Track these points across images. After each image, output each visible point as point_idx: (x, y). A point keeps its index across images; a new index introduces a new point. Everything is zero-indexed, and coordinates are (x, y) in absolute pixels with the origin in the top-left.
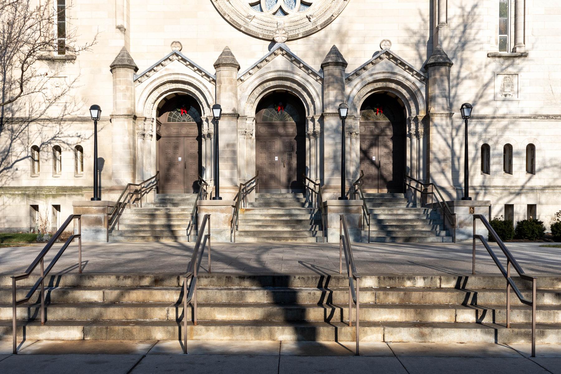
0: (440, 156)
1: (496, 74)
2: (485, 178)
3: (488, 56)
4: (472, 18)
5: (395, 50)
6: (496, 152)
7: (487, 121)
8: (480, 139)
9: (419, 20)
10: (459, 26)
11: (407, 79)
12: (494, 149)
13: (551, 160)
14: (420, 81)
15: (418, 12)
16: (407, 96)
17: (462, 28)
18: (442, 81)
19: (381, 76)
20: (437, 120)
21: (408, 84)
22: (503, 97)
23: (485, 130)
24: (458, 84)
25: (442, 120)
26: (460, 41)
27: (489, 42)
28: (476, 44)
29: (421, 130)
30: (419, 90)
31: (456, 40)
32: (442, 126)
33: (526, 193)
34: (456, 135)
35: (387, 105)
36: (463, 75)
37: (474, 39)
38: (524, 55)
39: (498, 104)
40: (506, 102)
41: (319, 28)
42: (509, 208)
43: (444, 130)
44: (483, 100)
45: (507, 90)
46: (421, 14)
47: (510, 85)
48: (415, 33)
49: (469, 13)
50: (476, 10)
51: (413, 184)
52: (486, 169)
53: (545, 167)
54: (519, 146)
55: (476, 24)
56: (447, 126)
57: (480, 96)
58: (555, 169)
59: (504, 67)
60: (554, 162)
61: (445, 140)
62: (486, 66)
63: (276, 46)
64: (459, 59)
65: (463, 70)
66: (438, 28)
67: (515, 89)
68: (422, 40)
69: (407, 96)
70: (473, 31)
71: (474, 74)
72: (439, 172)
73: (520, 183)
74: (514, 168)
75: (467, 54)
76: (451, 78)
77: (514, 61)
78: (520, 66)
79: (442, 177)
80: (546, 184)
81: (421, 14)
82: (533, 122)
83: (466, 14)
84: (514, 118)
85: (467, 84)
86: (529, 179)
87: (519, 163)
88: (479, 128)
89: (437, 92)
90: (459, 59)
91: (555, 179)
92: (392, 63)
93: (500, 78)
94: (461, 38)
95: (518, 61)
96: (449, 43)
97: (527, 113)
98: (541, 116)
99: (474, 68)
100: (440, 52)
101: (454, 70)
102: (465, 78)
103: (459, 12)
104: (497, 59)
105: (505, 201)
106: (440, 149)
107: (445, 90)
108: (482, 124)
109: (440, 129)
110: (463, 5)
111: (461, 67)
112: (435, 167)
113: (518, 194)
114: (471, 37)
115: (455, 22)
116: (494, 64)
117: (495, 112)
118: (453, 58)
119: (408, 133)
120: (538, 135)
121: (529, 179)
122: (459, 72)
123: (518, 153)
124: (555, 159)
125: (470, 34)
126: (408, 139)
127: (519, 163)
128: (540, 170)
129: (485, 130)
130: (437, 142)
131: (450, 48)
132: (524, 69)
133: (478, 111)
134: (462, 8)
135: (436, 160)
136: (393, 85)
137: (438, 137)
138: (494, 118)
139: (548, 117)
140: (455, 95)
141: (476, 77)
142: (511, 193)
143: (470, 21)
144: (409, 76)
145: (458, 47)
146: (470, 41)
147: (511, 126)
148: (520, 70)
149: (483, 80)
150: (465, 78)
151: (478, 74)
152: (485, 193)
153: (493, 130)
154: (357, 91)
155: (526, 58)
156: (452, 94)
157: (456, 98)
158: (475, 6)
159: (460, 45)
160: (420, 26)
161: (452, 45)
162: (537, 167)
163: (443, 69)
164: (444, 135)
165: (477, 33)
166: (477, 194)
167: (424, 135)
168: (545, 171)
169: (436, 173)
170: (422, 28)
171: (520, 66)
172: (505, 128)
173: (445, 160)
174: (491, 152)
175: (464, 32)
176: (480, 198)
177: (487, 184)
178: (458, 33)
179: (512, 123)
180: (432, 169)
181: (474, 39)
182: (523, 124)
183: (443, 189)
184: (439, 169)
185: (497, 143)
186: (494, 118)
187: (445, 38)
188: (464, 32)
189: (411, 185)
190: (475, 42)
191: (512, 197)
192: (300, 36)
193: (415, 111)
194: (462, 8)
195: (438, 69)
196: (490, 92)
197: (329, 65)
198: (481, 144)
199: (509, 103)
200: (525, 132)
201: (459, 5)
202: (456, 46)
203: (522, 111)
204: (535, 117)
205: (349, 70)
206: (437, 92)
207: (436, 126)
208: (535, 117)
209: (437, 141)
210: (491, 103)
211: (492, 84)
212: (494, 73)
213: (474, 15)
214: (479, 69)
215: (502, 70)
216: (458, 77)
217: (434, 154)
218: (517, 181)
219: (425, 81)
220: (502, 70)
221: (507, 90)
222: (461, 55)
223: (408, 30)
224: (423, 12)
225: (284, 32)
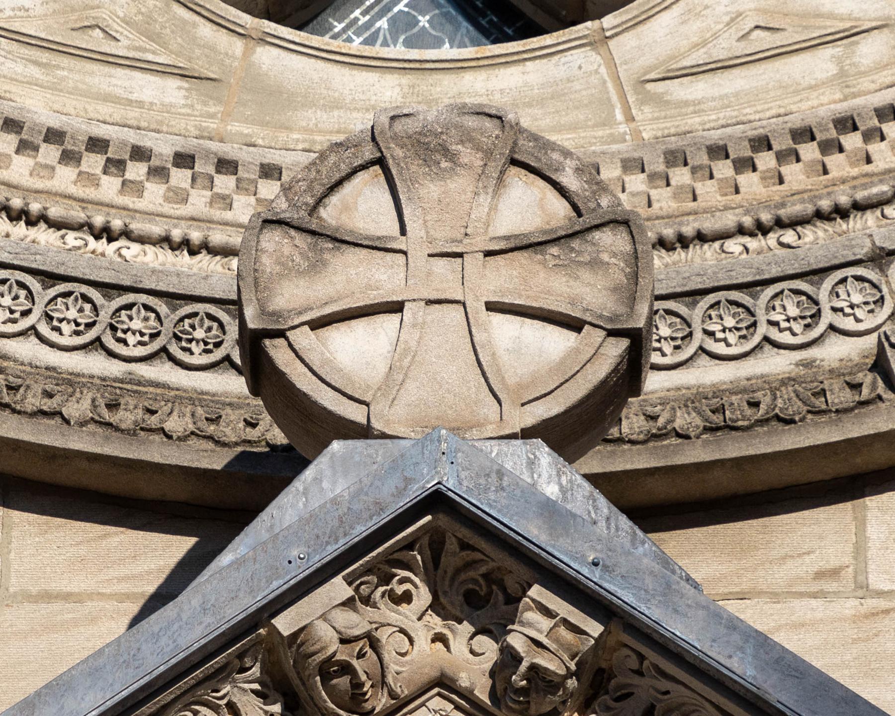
63: (328, 495)
225: (526, 206)
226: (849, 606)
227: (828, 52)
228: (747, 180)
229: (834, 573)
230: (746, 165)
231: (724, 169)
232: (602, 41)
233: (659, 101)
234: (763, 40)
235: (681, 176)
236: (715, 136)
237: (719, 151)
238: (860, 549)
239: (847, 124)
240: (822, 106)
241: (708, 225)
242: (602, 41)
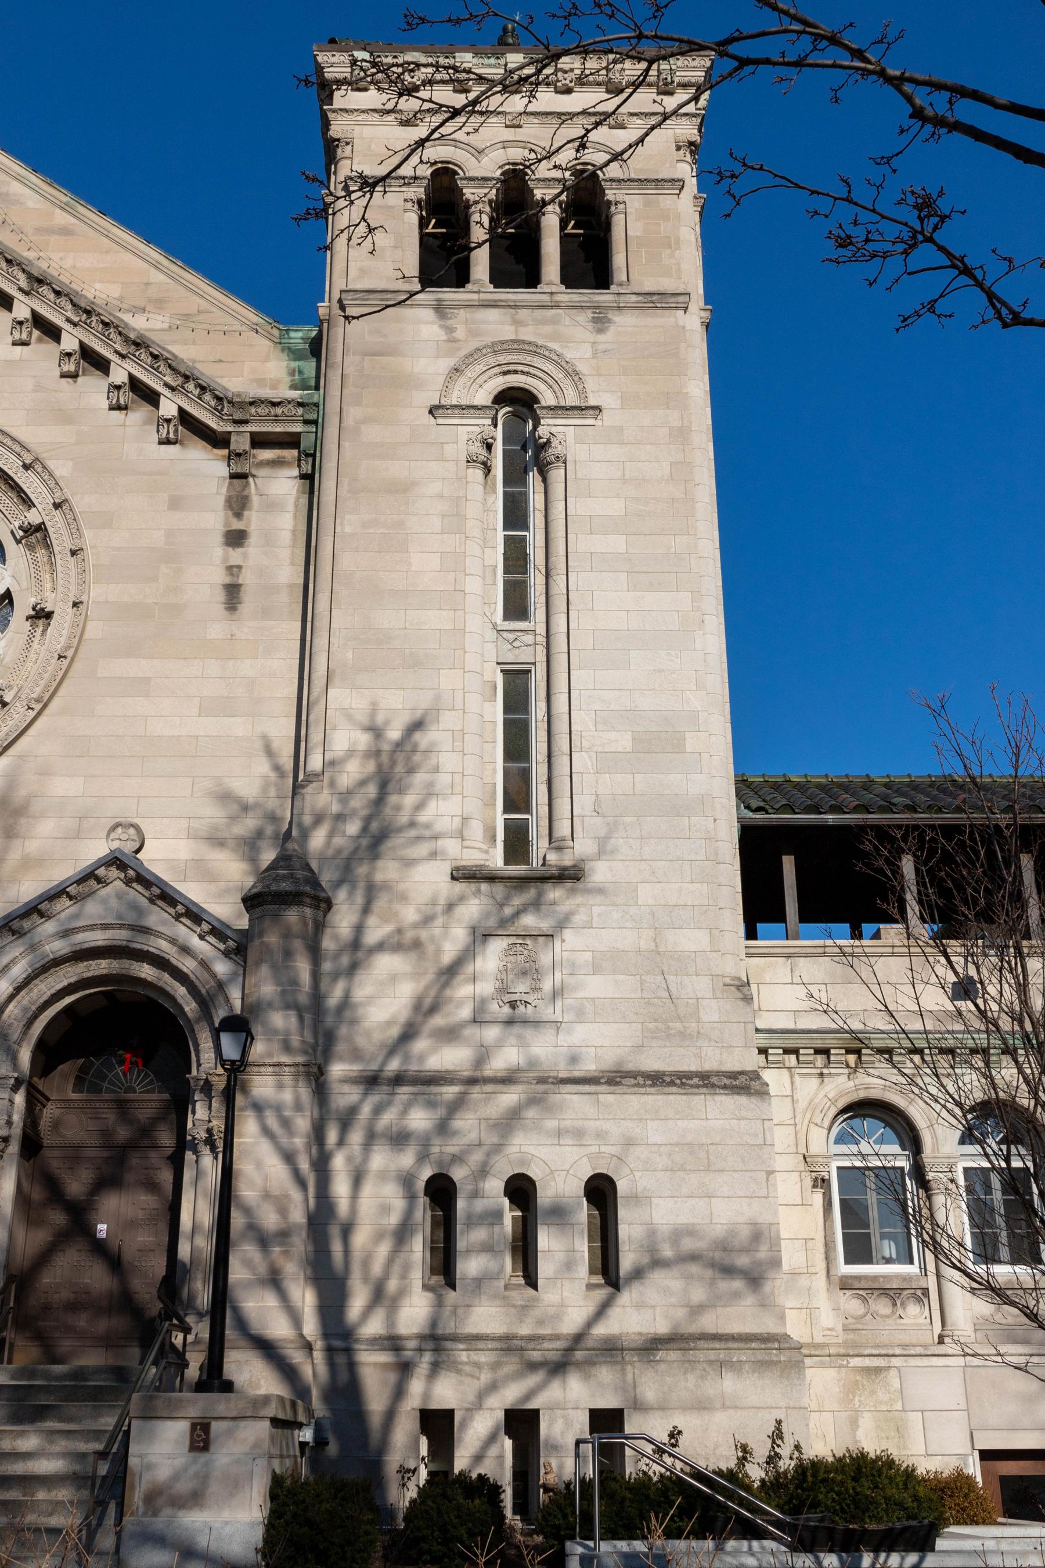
0: (270, 1220)
1: (481, 936)
2: (439, 1303)
3: (453, 878)
4: (408, 759)
5: (159, 857)
6: (480, 1205)
7: (450, 1091)
8: (423, 1157)
10: (363, 783)
12: (475, 1194)
13: (677, 1234)
14: (227, 954)
15: (259, 744)
16: (190, 1007)
17: (372, 791)
18: (288, 954)
19: (97, 938)
20: (261, 1085)
22: (506, 1009)
23: (443, 1128)
24: (353, 968)
25: (280, 1086)
26: (365, 829)
27: (460, 835)
28: (419, 838)
30: (221, 986)
31: (353, 828)
32: (278, 1108)
33: (590, 1363)
34: (341, 1143)
36: (374, 934)
37: (412, 824)
38: (570, 876)
39: (491, 1033)
40: (516, 1029)
42: (522, 1424)
43: (286, 1123)
44: (438, 1021)
45: (521, 987)
47: (530, 971)
48: (245, 808)
49: (399, 745)
50: (417, 736)
52: (444, 1265)
53: (658, 1263)
54: (561, 1179)
55: (419, 779)
56: (298, 1107)
57: (425, 1008)
58: (694, 1268)
59: (508, 911)
60: (688, 1245)
61: (289, 1157)
62: (450, 907)
65: (372, 921)
67: (547, 985)
68: (269, 830)
69: (190, 1007)
70: (409, 800)
71: (409, 935)
73: (572, 1321)
74: (545, 1268)
75: (387, 870)
76: (328, 944)
77: (540, 895)
78: (563, 908)
79: (270, 1300)
80: (662, 1328)
81: (269, 752)
82: (608, 1098)
83: (386, 747)
84: (542, 1081)
85: (385, 964)
86: (602, 1311)
87: (563, 1249)
88: (419, 1120)
89: (267, 989)
90: (362, 885)
91: (696, 1310)
92: (137, 895)
93: (497, 946)
94: (368, 820)
95: (554, 893)
97: (589, 1066)
98: (633, 1075)
99: (410, 914)
101: (343, 919)
102: (380, 947)
103: (363, 740)
104: (484, 887)
105: (510, 1395)
106: (267, 1195)
107: (295, 982)
108: (431, 1104)
109: (272, 1122)
110: (380, 719)
111: (366, 910)
112: (248, 1263)
113: (558, 1368)
114: (403, 819)
115: (352, 772)
116: (474, 907)
117: (480, 1061)
118: (338, 884)
120: (629, 1143)
121: (602, 1311)
122: (359, 929)
123: (559, 1213)
124: (690, 1231)
125: (398, 808)
127: (563, 1249)
128: (638, 1274)
129: (443, 1128)
130: (263, 1168)
131: (330, 852)
132: (578, 919)
133: (422, 1058)
134: (376, 731)
136: (146, 971)
137: (266, 1151)
138: (472, 1081)
139: (657, 1079)
140: (346, 1003)
141: (417, 945)
142: (533, 1366)
143: (399, 768)
144: (195, 942)
145: (356, 850)
146: (400, 830)
147: (531, 1113)
148: (562, 924)
149: (438, 952)
150: (380, 947)
151: (424, 934)
152: (435, 1368)
153: (468, 1125)
155: (580, 885)
156: (333, 1000)
157: (347, 1014)
158: (417, 726)
159: (365, 842)
160: (265, 789)
161: (338, 841)
162: (627, 1261)
163: (292, 916)
164: (284, 1140)
165: (420, 807)
166: (405, 1369)
168: (659, 1278)
169: (248, 1285)
170: (272, 792)
171: (563, 908)
172: (512, 1119)
173: (284, 1235)
174: (461, 1204)
175: (380, 801)
176: (416, 1386)
177: (448, 1327)
178: (358, 804)
179: (533, 1101)
180: (237, 1272)
181: (412, 824)
182: (575, 1104)
184: (262, 1269)
185: (483, 1172)
186: (472, 1081)
187: (318, 820)
188: (380, 801)
190: (413, 833)
191: (533, 1380)
194: (376, 731)
195: (276, 916)
196: (464, 994)
198: (427, 1173)
199: (529, 1033)
200: (578, 1134)
201: (365, 721)
202: (351, 846)
203: (574, 1059)
204: (615, 1078)
206: (267, 989)
207: (258, 1108)
208: (615, 1078)
210: (467, 1032)
211: (469, 969)
212: (474, 930)
213: (414, 751)
214: (427, 920)
215: (503, 922)
216: (355, 944)
217: (247, 1211)
218: (557, 1317)
220: (503, 922)
221: (521, 987)
224: (275, 745)
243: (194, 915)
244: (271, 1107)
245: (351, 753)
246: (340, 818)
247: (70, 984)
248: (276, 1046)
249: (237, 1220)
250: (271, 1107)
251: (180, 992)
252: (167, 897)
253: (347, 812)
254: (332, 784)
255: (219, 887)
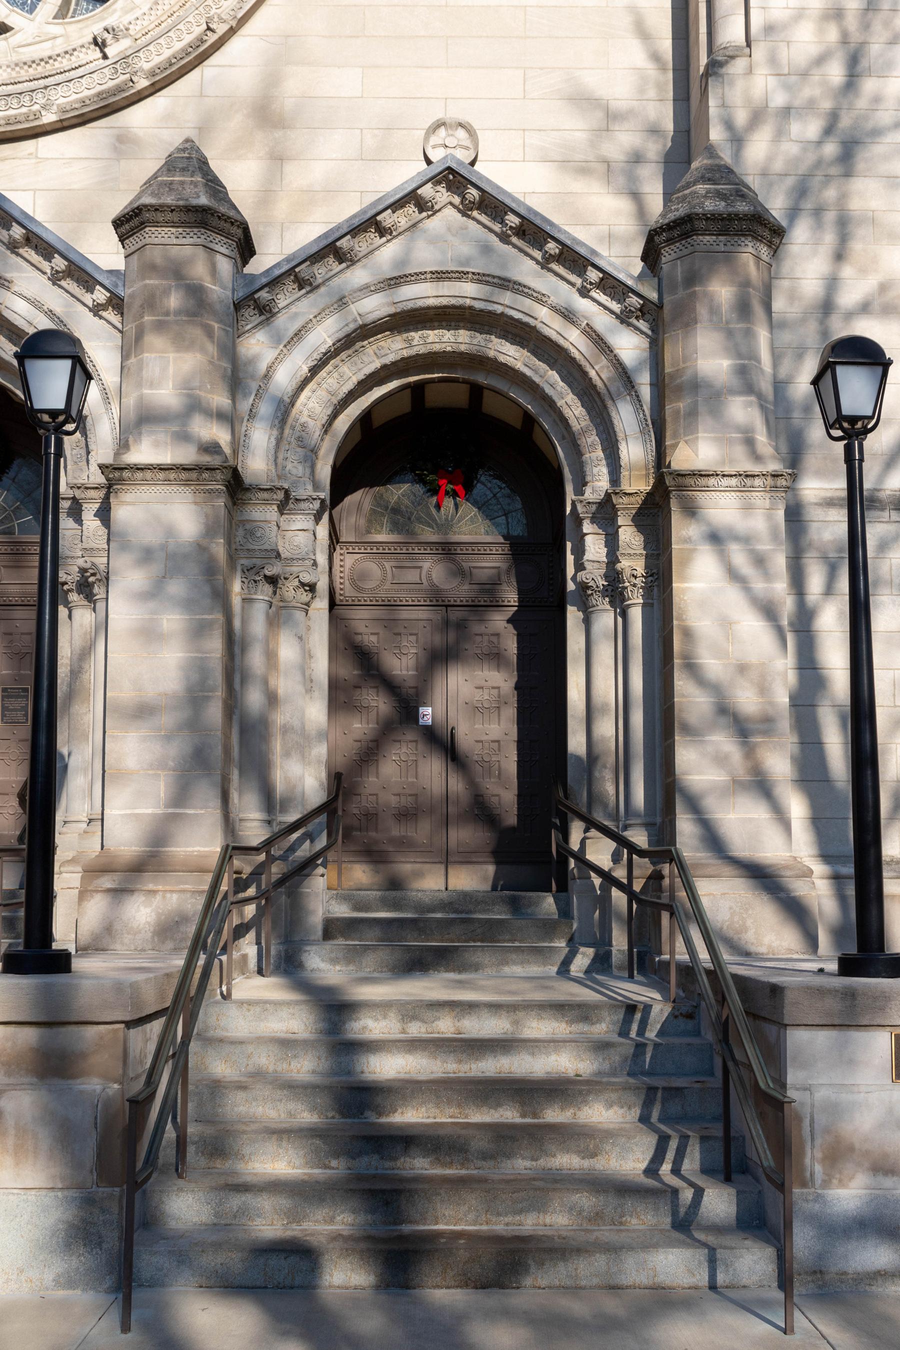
9: (635, 55)
10: (821, 60)
11: (568, 315)
17: (836, 73)
21: (574, 340)
25: (747, 508)
26: (829, 131)
29: (633, 564)
31: (812, 129)
32: (746, 540)
35: (460, 441)
41: (142, 83)
46: (643, 32)
51: (601, 852)
64: (830, 216)
66: (715, 67)
72: (737, 786)
75: (867, 194)
90: (830, 216)
94: (833, 118)
96: (780, 134)
100: (724, 175)
109: (739, 557)
114: (884, 117)
115: (805, 41)
119: (571, 586)
126: (573, 615)
131: (778, 166)
135: (723, 720)
145: (819, 163)
146: (877, 133)
154: (312, 373)
159: (831, 149)
161: (790, 149)
167: (648, 590)
183: (762, 877)
187: (757, 117)
189: (591, 856)
192: (49, 118)
193: (611, 467)
197: (142, 225)
202: (811, 158)
205: (269, 256)
209: (726, 624)
219: (657, 318)
222: (843, 197)
223: (582, 100)
226: (34, 161)
227: (50, 42)
228: (31, 70)
229: (31, 154)
230: (30, 66)
231: (26, 67)
232: (6, 39)
233: (17, 52)
234: (38, 39)
235: (17, 69)
236: (24, 60)
237: (25, 63)
238: (37, 149)
239: (50, 58)
240: (45, 54)
241: (20, 80)
242: (6, 39)
243: (573, 259)
244: (737, 538)
245: (800, 14)
246: (786, 112)
247: (384, 367)
248: (739, 451)
249: (690, 699)
250: (737, 538)
251: (552, 381)
252: (531, 232)
253: (797, 103)
254: (773, 60)
255: (608, 224)
